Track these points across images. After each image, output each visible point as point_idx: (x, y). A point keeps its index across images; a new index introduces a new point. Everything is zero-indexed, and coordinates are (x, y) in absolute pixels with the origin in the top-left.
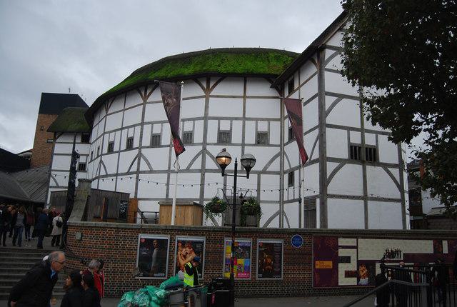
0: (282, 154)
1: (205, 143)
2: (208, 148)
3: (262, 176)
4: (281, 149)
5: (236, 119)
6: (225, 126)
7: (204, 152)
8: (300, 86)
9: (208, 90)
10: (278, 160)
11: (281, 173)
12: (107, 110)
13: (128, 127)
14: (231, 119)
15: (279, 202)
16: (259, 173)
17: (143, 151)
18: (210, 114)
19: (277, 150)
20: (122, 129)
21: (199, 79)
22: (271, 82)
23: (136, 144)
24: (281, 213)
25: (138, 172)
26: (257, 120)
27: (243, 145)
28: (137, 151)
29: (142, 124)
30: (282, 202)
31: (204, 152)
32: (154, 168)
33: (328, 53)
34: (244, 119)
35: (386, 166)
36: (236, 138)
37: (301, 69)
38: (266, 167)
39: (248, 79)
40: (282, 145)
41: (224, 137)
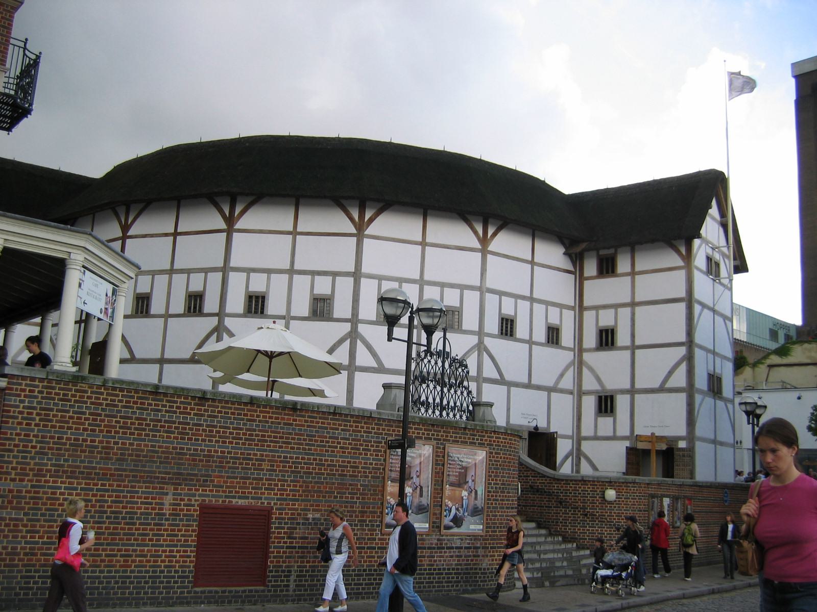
0: (580, 364)
1: (481, 333)
2: (488, 341)
3: (553, 394)
4: (574, 355)
5: (523, 298)
7: (480, 347)
8: (633, 273)
9: (484, 241)
10: (570, 375)
11: (580, 393)
12: (230, 221)
13: (314, 273)
14: (517, 297)
15: (571, 437)
16: (550, 390)
17: (361, 328)
18: (489, 284)
19: (569, 356)
20: (292, 271)
23: (342, 308)
24: (578, 454)
25: (352, 368)
26: (547, 303)
27: (530, 342)
28: (347, 327)
29: (357, 275)
30: (579, 439)
31: (480, 347)
32: (387, 366)
33: (696, 242)
34: (532, 299)
35: (726, 400)
36: (521, 330)
37: (637, 247)
39: (536, 232)
40: (580, 349)
41: (507, 327)
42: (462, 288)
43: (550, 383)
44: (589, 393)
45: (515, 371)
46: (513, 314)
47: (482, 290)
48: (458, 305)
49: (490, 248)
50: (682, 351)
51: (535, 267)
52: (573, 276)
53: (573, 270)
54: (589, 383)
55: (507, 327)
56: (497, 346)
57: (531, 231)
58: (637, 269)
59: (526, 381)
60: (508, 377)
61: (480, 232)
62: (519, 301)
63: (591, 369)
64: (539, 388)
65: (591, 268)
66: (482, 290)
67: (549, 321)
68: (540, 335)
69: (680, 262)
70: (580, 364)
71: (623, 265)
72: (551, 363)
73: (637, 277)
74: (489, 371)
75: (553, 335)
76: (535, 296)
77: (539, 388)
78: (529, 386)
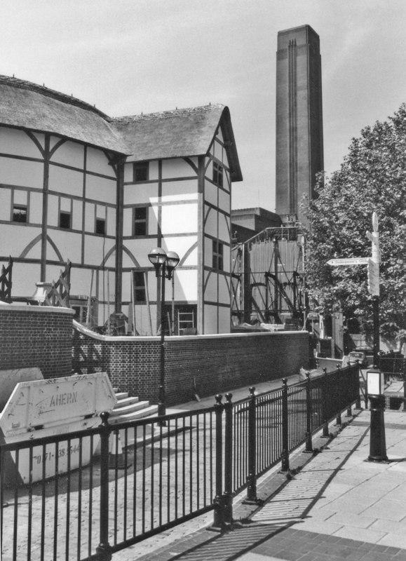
0: (119, 249)
1: (44, 226)
2: (50, 232)
3: (101, 272)
5: (77, 198)
6: (66, 207)
7: (44, 237)
11: (119, 270)
14: (73, 197)
16: (98, 268)
21: (35, 134)
22: (109, 158)
27: (83, 233)
31: (44, 237)
33: (207, 159)
34: (84, 200)
35: (225, 274)
36: (76, 223)
38: (104, 263)
39: (88, 148)
40: (119, 238)
41: (65, 222)
42: (29, 190)
43: (98, 263)
44: (128, 270)
45: (72, 255)
46: (69, 211)
47: (46, 192)
48: (23, 202)
49: (51, 160)
50: (194, 239)
51: (87, 175)
52: (115, 182)
53: (115, 177)
54: (127, 262)
55: (65, 222)
56: (57, 236)
57: (83, 146)
58: (163, 177)
59: (80, 262)
60: (65, 260)
61: (43, 147)
62: (74, 201)
63: (128, 252)
64: (89, 267)
65: (129, 175)
66: (46, 192)
67: (98, 216)
68: (91, 226)
69: (193, 173)
70: (119, 249)
71: (153, 174)
72: (98, 249)
73: (163, 184)
74: (51, 255)
75: (100, 228)
76: (87, 197)
77: (89, 267)
78: (82, 266)
